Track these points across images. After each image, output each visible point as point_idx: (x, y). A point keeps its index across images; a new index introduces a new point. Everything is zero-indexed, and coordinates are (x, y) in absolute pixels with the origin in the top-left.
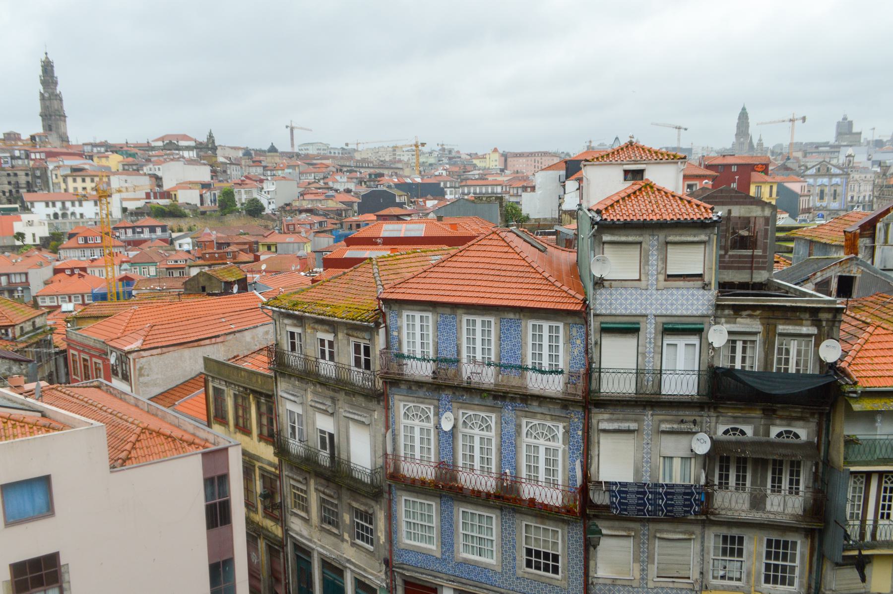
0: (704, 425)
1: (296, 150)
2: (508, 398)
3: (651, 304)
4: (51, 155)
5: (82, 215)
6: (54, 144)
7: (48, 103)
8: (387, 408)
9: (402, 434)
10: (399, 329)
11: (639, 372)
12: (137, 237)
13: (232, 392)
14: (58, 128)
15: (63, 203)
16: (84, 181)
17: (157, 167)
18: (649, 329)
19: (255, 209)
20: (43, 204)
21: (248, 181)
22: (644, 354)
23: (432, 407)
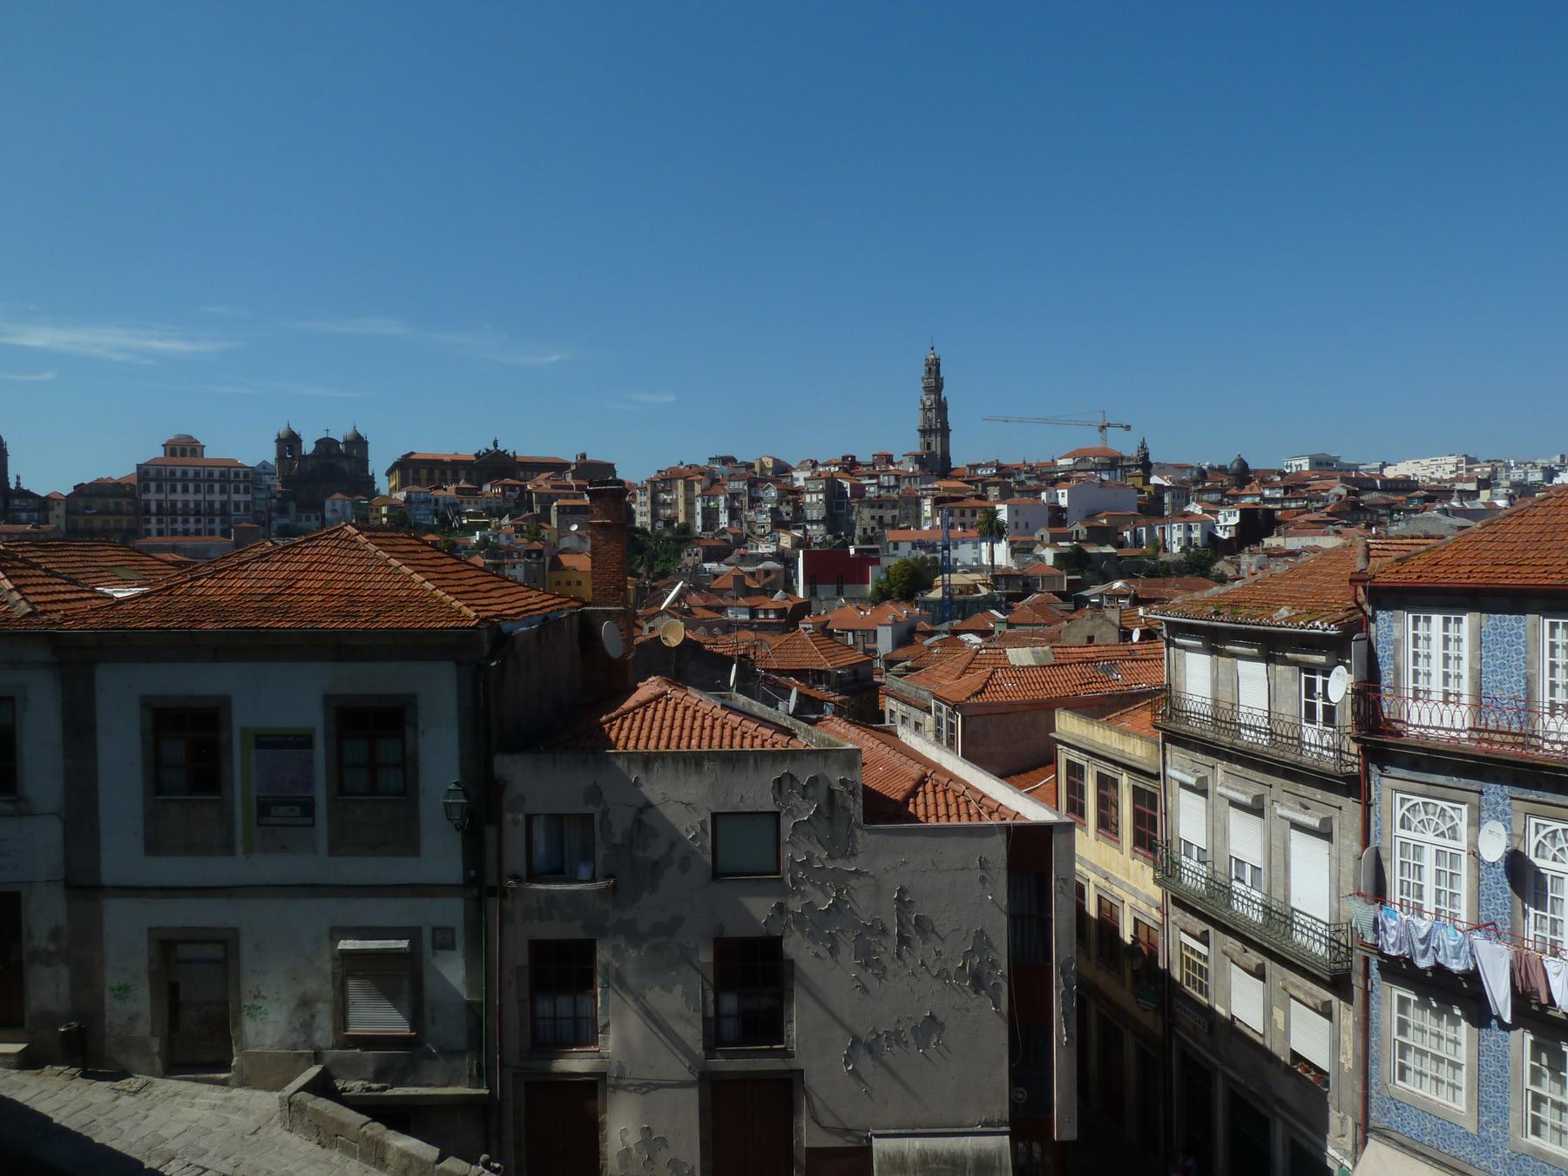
5: (956, 560)
10: (1397, 644)
13: (1095, 769)
16: (963, 514)
20: (909, 545)
23: (1464, 808)
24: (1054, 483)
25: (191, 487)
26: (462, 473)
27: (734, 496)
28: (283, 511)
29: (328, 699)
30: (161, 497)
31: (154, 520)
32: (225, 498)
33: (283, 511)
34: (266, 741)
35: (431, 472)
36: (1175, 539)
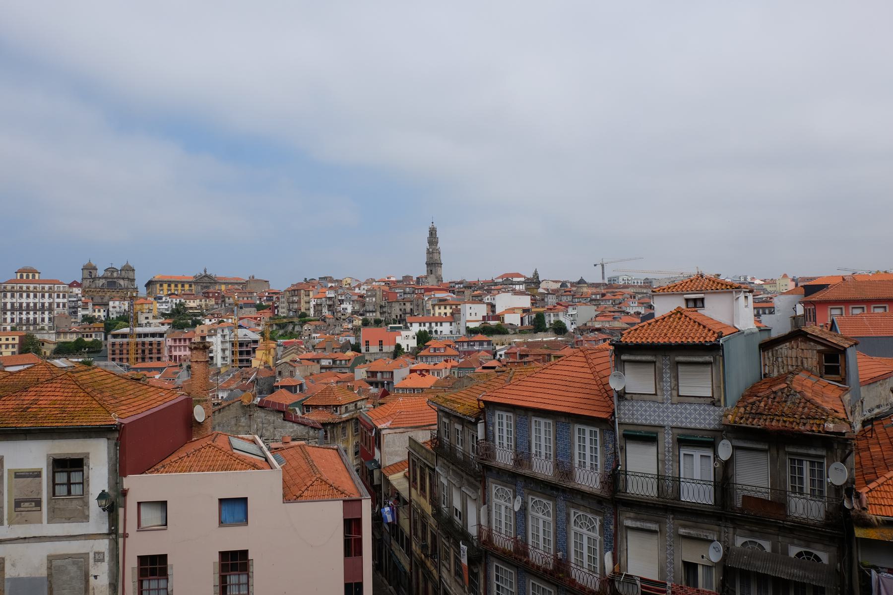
0: (723, 534)
1: (607, 282)
2: (559, 490)
3: (668, 416)
4: (428, 290)
6: (432, 282)
8: (484, 488)
9: (494, 510)
11: (660, 478)
12: (470, 348)
15: (430, 324)
18: (667, 439)
19: (560, 329)
21: (559, 307)
22: (664, 461)
24: (489, 291)
25: (32, 295)
26: (187, 287)
27: (330, 298)
28: (85, 307)
29: (48, 456)
30: (14, 300)
31: (9, 313)
32: (51, 300)
33: (85, 307)
34: (18, 475)
35: (169, 286)
36: (547, 320)
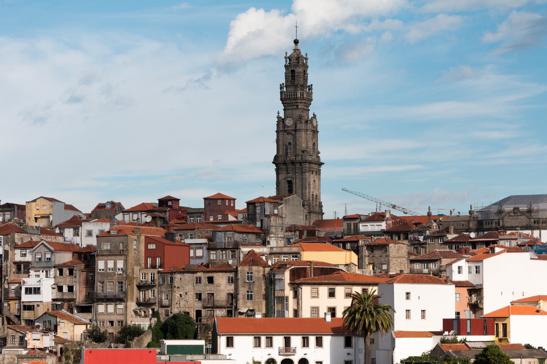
7: (289, 138)
14: (303, 187)
16: (332, 294)
17: (473, 265)
20: (250, 340)
